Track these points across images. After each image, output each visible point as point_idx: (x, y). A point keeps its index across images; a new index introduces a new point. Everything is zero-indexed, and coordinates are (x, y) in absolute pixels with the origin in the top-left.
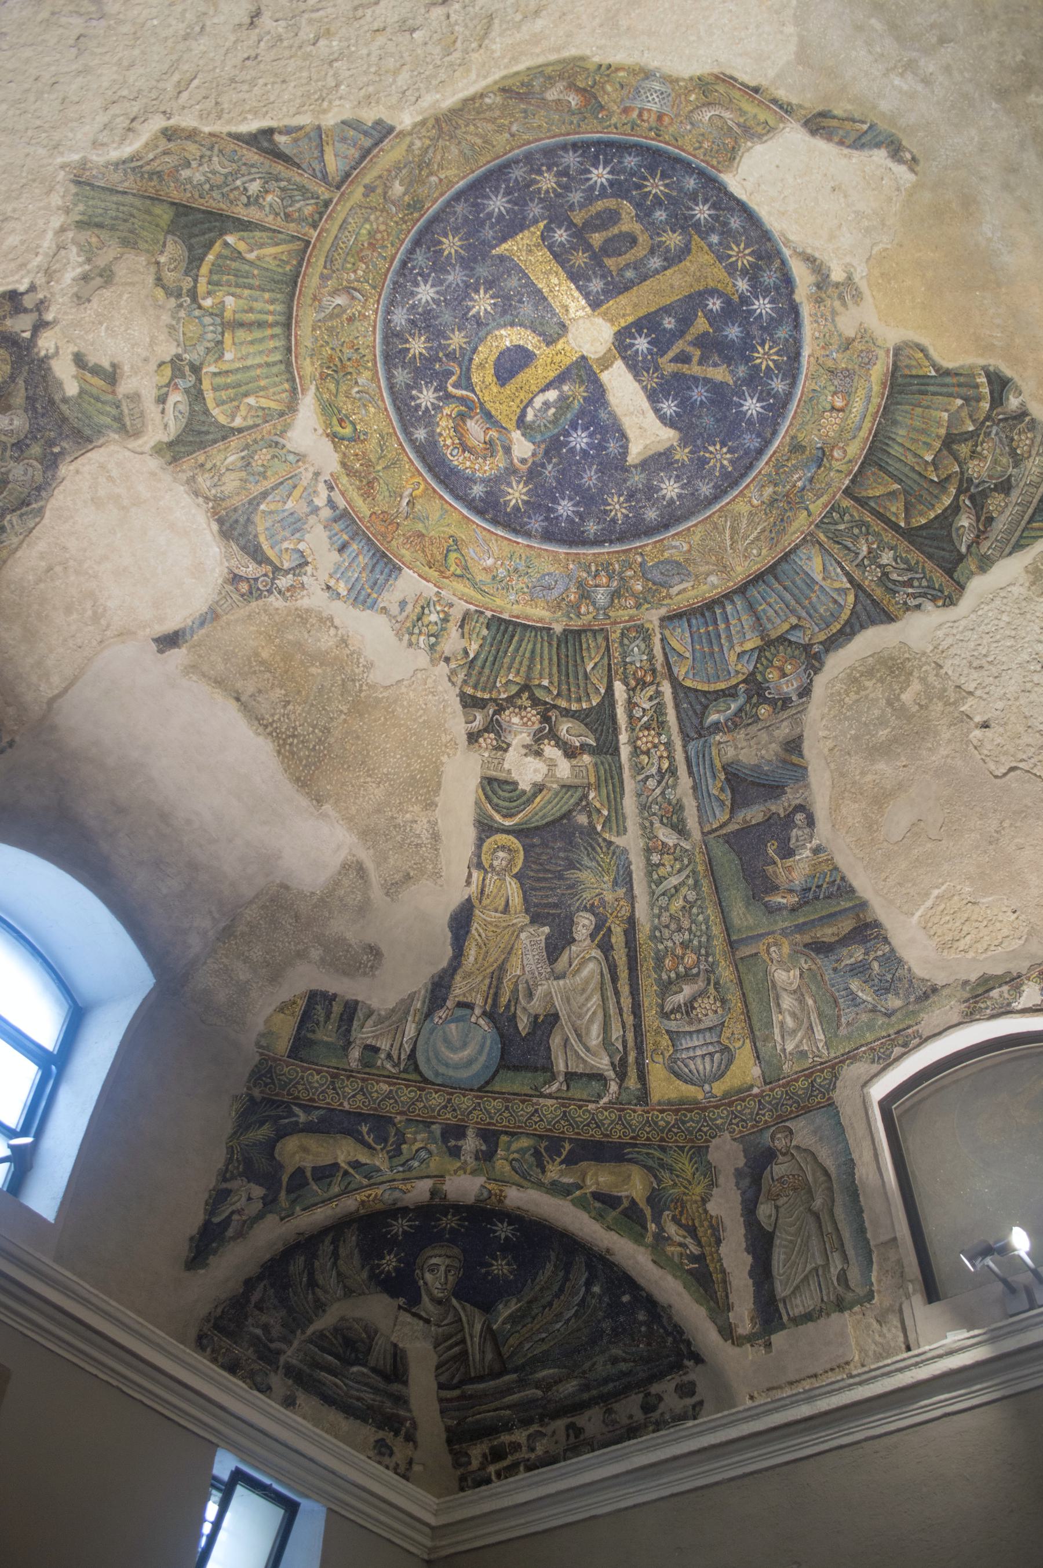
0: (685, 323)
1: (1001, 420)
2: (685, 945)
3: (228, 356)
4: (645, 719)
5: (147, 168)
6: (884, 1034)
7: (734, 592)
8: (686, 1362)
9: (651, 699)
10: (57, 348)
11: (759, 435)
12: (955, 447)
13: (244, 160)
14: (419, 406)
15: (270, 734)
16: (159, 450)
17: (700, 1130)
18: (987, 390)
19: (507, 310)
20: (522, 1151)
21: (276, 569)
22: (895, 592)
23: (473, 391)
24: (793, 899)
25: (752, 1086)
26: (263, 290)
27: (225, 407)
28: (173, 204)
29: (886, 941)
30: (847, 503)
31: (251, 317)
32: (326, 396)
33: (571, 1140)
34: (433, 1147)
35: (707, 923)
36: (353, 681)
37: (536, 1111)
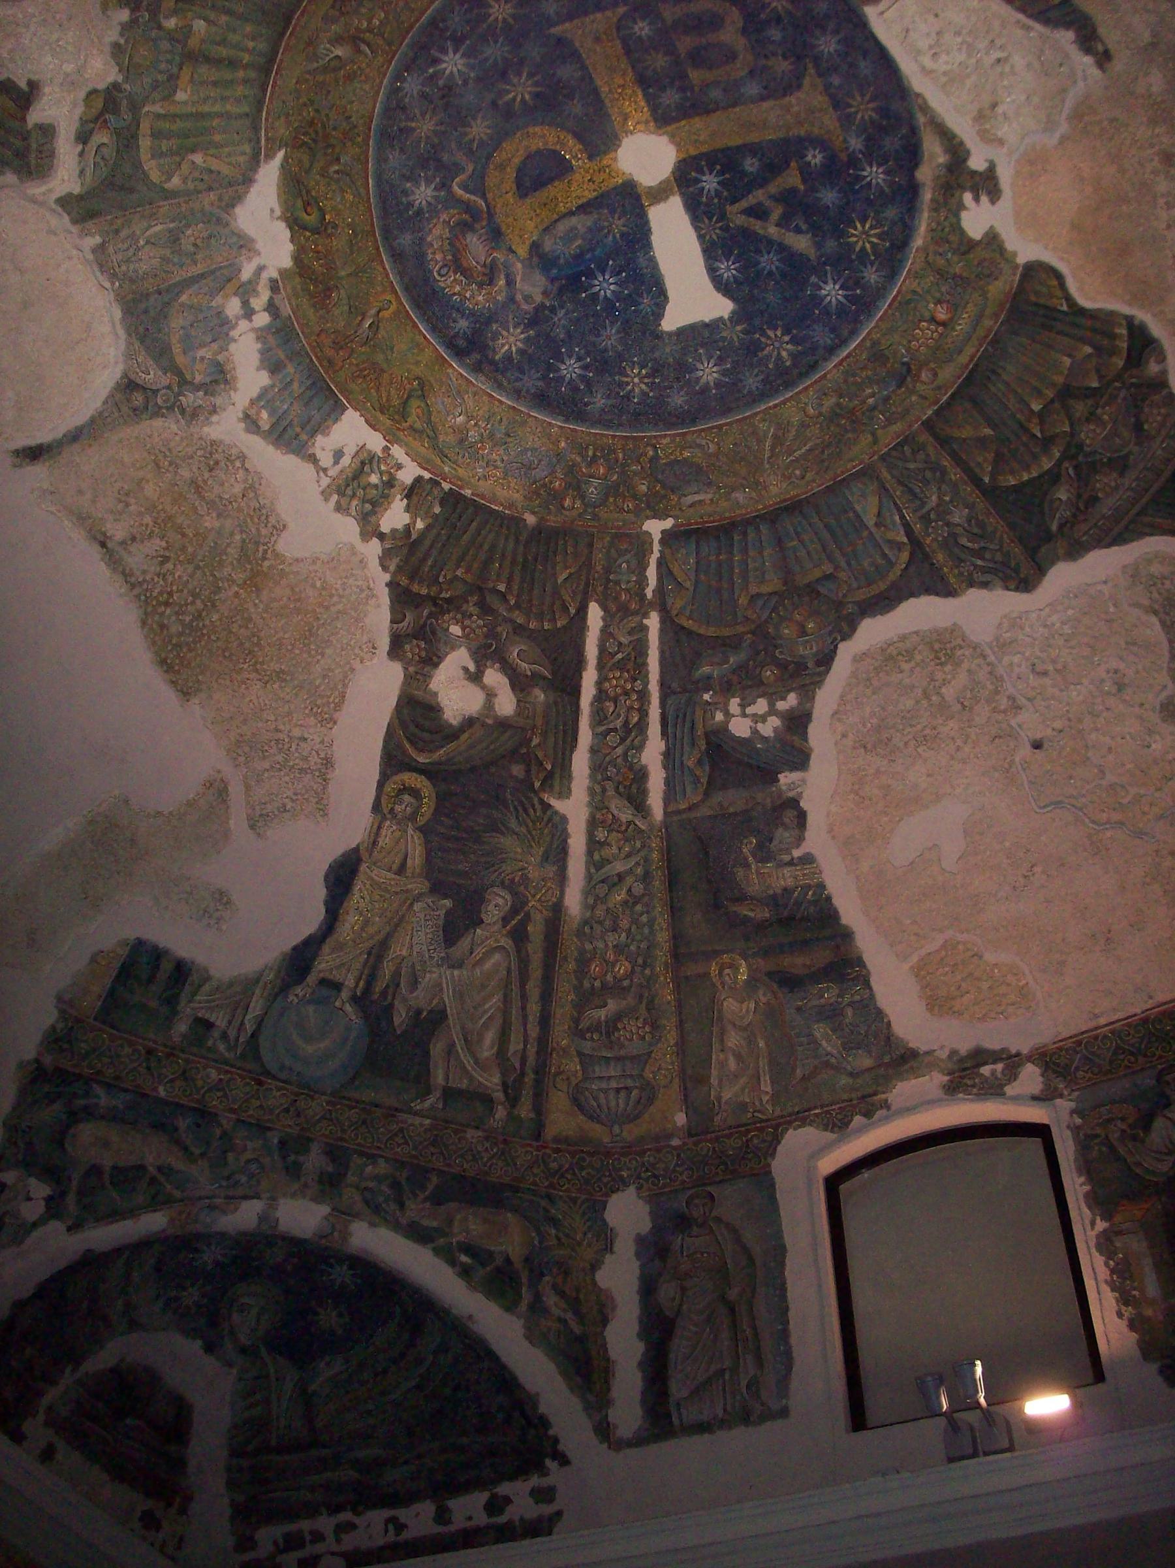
0: (772, 169)
1: (1132, 384)
2: (619, 949)
3: (181, 96)
4: (620, 656)
6: (845, 1097)
7: (761, 517)
8: (548, 1462)
9: (629, 633)
11: (833, 330)
12: (1072, 402)
14: (410, 205)
15: (138, 596)
16: (65, 202)
17: (599, 1179)
18: (1125, 345)
19: (547, 104)
20: (377, 1178)
21: (183, 382)
22: (962, 561)
23: (484, 196)
24: (764, 914)
25: (670, 1136)
26: (247, 20)
27: (162, 161)
29: (867, 985)
30: (924, 437)
31: (224, 52)
33: (441, 1173)
34: (266, 1161)
35: (651, 927)
36: (257, 543)
37: (401, 1130)
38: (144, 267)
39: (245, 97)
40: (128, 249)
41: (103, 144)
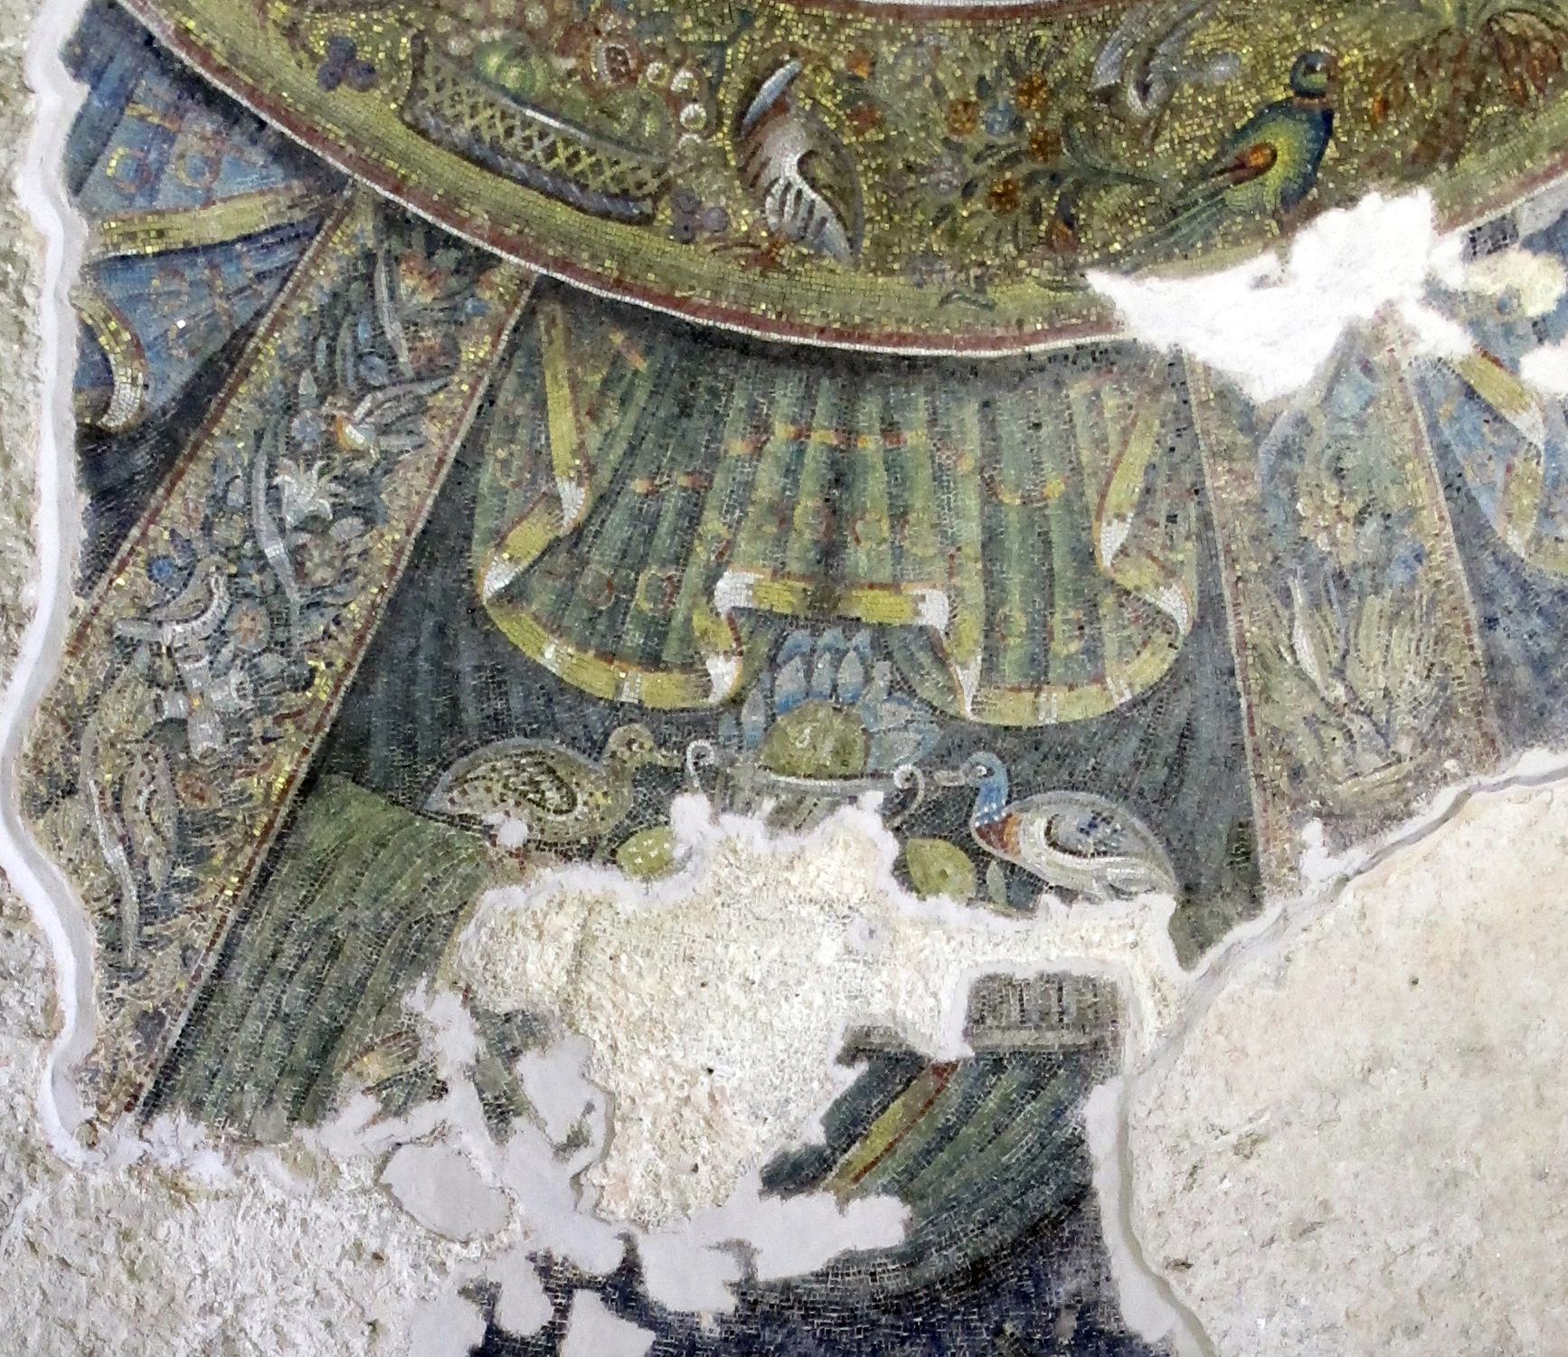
3: (934, 612)
5: (156, 867)
10: (726, 1247)
13: (190, 532)
16: (1193, 936)
26: (714, 458)
27: (1110, 649)
28: (310, 786)
31: (808, 505)
32: (1138, 228)
38: (1410, 680)
39: (933, 422)
40: (1349, 736)
41: (1048, 832)
